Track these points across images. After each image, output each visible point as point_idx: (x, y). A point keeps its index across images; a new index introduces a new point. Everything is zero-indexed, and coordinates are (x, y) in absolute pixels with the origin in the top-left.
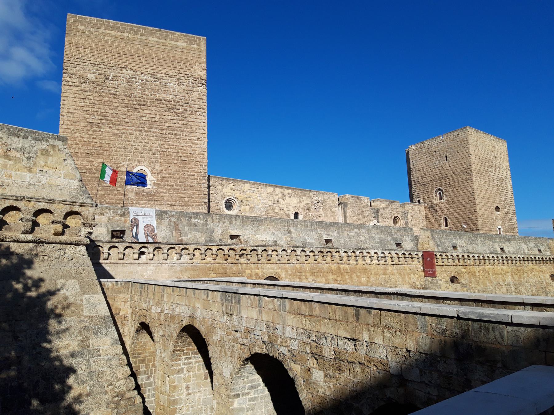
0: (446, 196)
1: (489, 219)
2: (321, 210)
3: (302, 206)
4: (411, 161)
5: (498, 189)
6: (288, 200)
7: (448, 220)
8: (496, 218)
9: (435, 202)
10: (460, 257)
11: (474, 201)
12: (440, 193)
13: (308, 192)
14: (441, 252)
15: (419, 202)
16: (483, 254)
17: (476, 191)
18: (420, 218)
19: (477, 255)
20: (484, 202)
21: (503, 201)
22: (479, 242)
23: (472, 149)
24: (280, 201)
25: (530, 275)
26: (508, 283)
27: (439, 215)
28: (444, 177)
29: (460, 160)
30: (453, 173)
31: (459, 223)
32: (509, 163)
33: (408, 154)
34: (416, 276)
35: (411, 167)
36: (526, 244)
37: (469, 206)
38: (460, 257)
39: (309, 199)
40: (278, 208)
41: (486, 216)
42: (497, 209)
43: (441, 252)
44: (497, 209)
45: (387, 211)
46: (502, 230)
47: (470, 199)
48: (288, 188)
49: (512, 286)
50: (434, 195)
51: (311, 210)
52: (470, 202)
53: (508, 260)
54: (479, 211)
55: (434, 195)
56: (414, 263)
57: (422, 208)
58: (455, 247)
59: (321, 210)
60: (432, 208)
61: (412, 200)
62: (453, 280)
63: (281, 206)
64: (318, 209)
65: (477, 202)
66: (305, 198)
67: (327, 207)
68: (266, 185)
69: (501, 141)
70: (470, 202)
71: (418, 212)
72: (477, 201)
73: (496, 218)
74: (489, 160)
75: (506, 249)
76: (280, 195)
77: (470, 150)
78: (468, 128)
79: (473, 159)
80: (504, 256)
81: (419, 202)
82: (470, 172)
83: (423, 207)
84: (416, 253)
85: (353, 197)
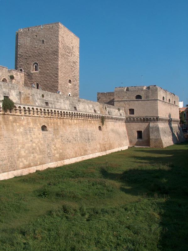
0: (40, 68)
1: (64, 87)
4: (19, 40)
5: (72, 69)
7: (39, 85)
8: (68, 87)
9: (32, 72)
10: (50, 111)
11: (57, 74)
12: (36, 66)
14: (38, 106)
15: (21, 70)
17: (59, 68)
18: (21, 82)
19: (60, 110)
20: (63, 75)
21: (73, 77)
22: (62, 101)
23: (60, 39)
25: (88, 127)
26: (76, 131)
27: (33, 81)
28: (40, 55)
29: (52, 45)
30: (46, 53)
31: (46, 88)
32: (79, 53)
33: (17, 35)
34: (18, 124)
35: (19, 44)
36: (88, 105)
37: (54, 77)
38: (50, 111)
41: (63, 85)
42: (70, 81)
43: (38, 106)
44: (70, 81)
46: (71, 95)
47: (55, 72)
49: (78, 133)
50: (32, 67)
52: (55, 74)
53: (77, 116)
54: (59, 81)
55: (32, 67)
56: (16, 114)
57: (23, 74)
58: (47, 103)
60: (29, 76)
61: (16, 68)
65: (59, 75)
69: (77, 38)
70: (55, 74)
71: (20, 77)
72: (59, 74)
73: (68, 87)
74: (69, 48)
75: (77, 109)
77: (59, 39)
78: (60, 24)
79: (60, 46)
80: (76, 112)
81: (21, 70)
82: (57, 54)
83: (24, 75)
84: (19, 106)
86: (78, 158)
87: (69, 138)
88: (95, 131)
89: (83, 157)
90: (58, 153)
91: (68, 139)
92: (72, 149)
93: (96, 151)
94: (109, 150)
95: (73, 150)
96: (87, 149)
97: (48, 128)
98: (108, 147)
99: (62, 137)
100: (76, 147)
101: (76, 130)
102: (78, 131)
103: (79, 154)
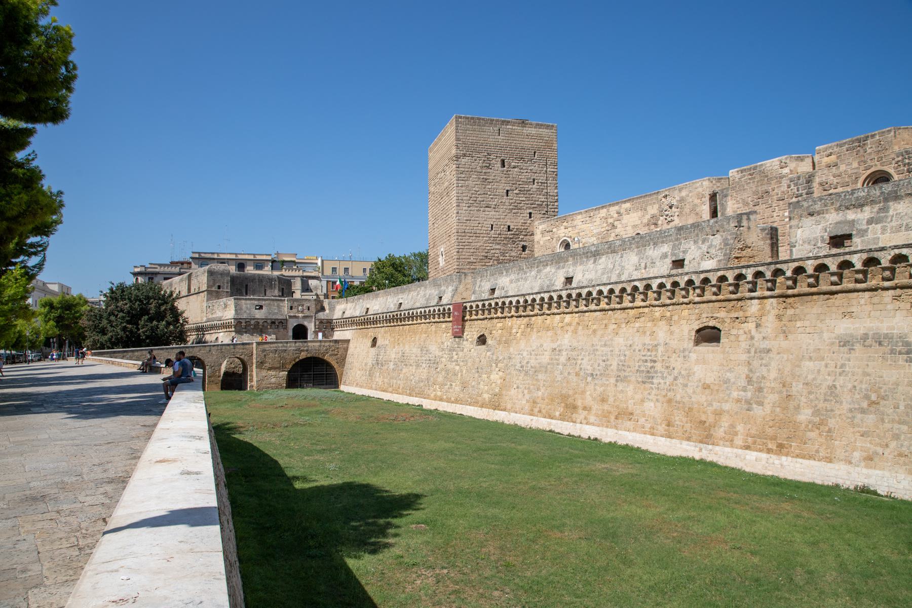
2: (676, 218)
3: (645, 221)
6: (626, 219)
13: (655, 196)
16: (524, 295)
24: (616, 223)
39: (656, 206)
40: (613, 235)
45: (843, 168)
48: (625, 202)
49: (564, 353)
51: (660, 222)
59: (676, 218)
62: (482, 340)
63: (617, 230)
64: (669, 219)
66: (649, 208)
67: (687, 210)
68: (599, 209)
76: (616, 215)
85: (742, 171)
86: (535, 418)
87: (528, 363)
88: (661, 349)
89: (554, 421)
90: (487, 392)
91: (522, 367)
92: (526, 391)
93: (629, 424)
94: (747, 448)
95: (527, 396)
96: (579, 403)
97: (489, 341)
98: (740, 428)
99: (510, 358)
100: (538, 389)
101: (559, 342)
102: (564, 347)
103: (544, 411)
